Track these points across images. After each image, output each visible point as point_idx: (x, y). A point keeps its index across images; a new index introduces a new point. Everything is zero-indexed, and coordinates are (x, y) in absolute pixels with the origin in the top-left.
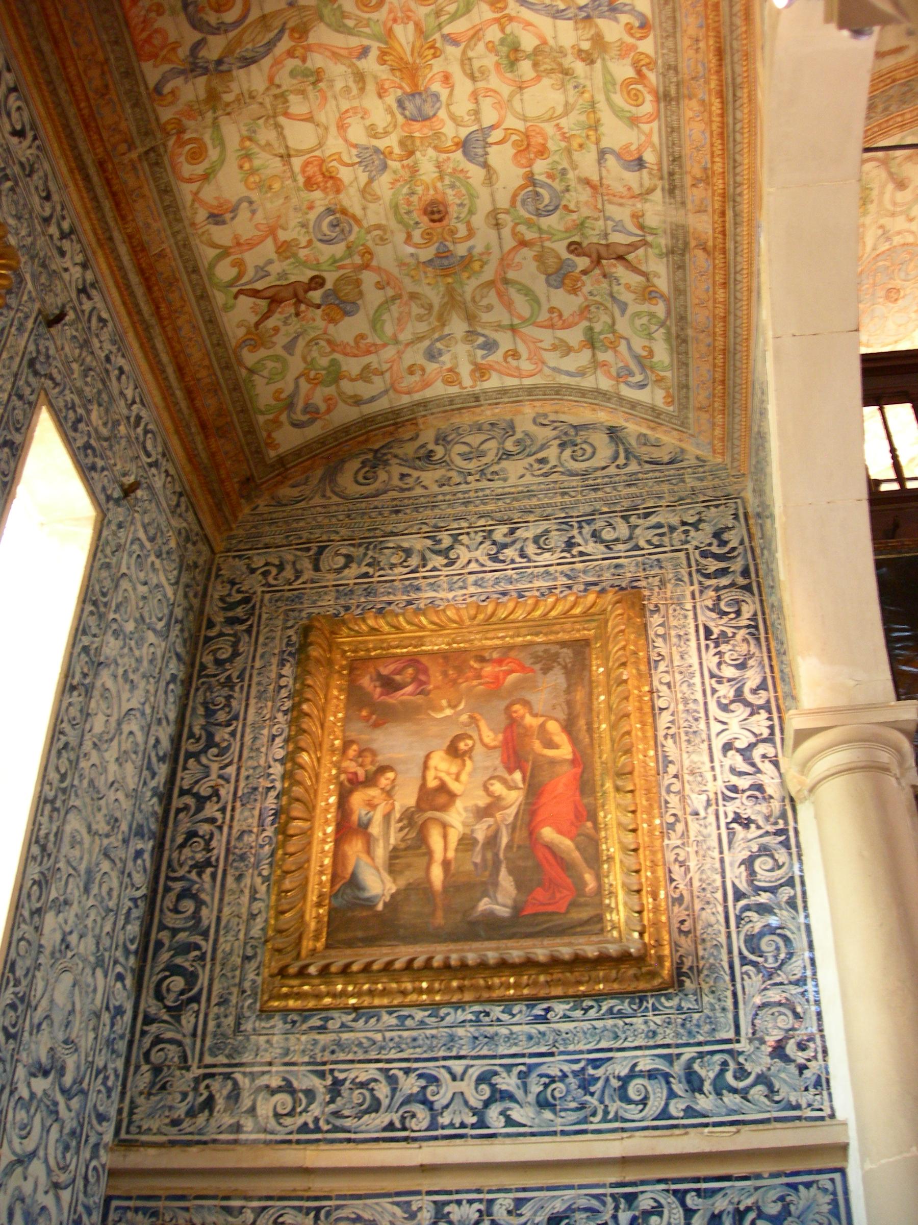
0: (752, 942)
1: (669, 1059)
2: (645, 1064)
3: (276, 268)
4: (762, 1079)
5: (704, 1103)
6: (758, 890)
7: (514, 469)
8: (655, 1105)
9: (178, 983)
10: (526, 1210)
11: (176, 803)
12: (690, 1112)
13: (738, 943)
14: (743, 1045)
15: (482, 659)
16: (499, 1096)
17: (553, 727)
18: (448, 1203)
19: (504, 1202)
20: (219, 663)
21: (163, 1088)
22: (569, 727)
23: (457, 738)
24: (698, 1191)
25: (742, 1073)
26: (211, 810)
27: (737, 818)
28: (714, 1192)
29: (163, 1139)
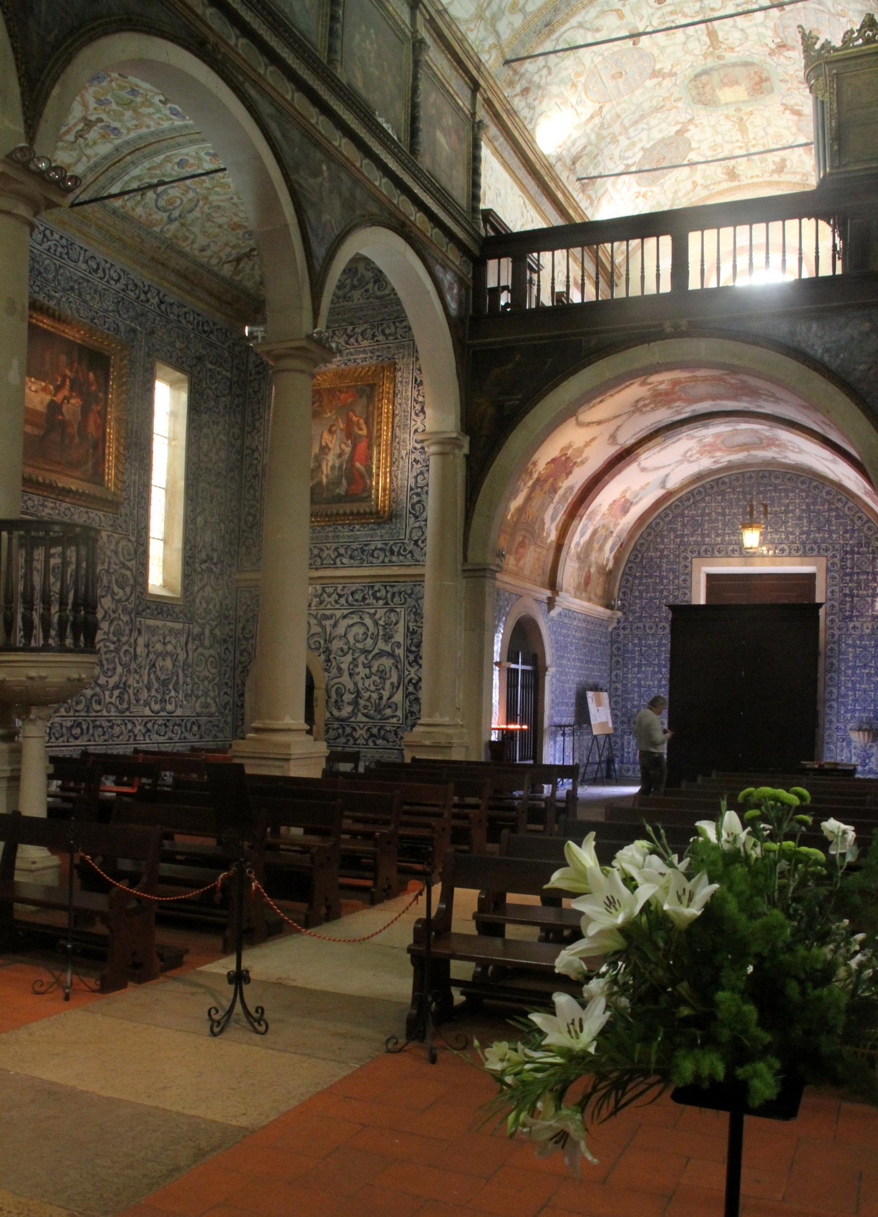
0: (413, 506)
1: (386, 544)
2: (379, 546)
3: (234, 252)
4: (411, 552)
5: (394, 558)
6: (417, 487)
7: (357, 294)
8: (381, 559)
9: (251, 518)
11: (246, 452)
12: (390, 561)
13: (409, 506)
14: (406, 541)
15: (340, 391)
16: (340, 555)
17: (362, 421)
19: (340, 587)
20: (255, 392)
22: (366, 423)
23: (332, 426)
25: (405, 550)
26: (256, 455)
27: (415, 460)
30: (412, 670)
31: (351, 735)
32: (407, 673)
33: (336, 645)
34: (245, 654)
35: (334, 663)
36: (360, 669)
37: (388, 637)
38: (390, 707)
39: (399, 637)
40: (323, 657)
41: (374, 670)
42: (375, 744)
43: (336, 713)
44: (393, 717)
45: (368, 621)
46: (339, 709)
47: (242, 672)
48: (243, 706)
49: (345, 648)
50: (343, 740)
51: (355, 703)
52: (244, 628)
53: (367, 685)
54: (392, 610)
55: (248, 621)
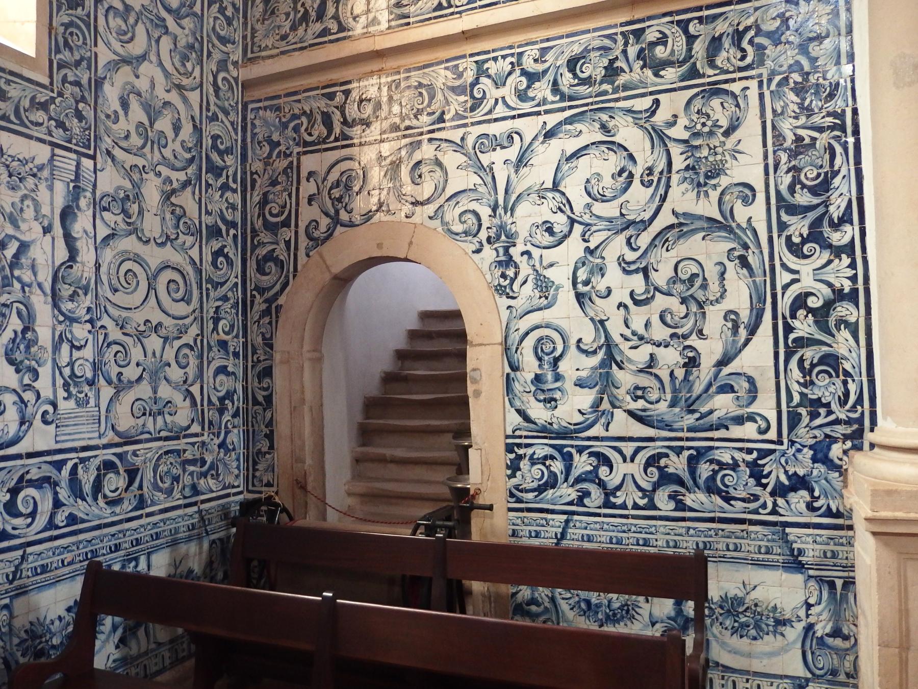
10: (550, 57)
18: (487, 61)
19: (532, 52)
21: (273, 13)
24: (700, 19)
28: (715, 17)
29: (277, 51)
30: (806, 268)
31: (592, 477)
32: (783, 278)
33: (527, 217)
34: (271, 266)
35: (525, 270)
36: (613, 276)
37: (703, 176)
38: (727, 388)
39: (747, 167)
40: (489, 254)
41: (661, 278)
42: (681, 506)
43: (539, 413)
44: (740, 420)
45: (629, 134)
46: (550, 402)
47: (267, 312)
48: (269, 399)
49: (560, 222)
50: (567, 492)
51: (603, 381)
52: (264, 201)
53: (638, 324)
54: (714, 91)
55: (274, 183)
